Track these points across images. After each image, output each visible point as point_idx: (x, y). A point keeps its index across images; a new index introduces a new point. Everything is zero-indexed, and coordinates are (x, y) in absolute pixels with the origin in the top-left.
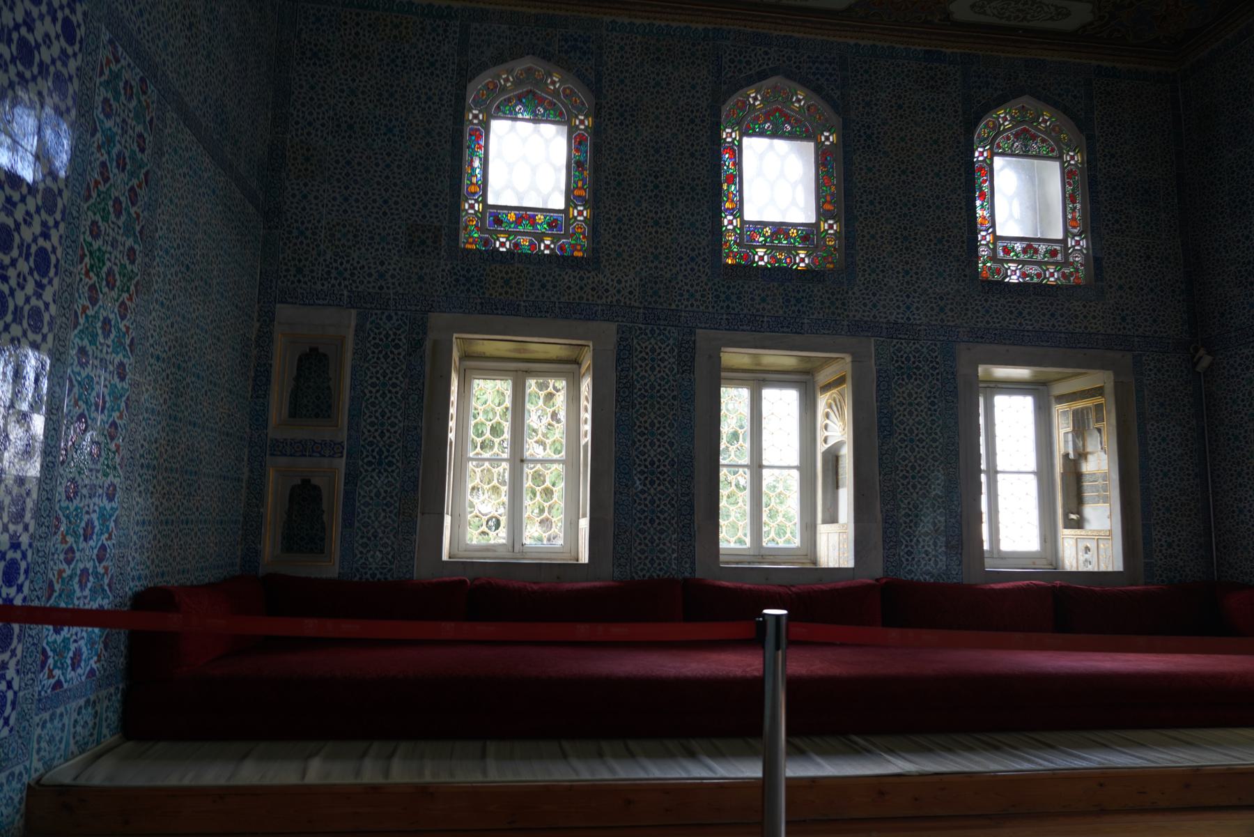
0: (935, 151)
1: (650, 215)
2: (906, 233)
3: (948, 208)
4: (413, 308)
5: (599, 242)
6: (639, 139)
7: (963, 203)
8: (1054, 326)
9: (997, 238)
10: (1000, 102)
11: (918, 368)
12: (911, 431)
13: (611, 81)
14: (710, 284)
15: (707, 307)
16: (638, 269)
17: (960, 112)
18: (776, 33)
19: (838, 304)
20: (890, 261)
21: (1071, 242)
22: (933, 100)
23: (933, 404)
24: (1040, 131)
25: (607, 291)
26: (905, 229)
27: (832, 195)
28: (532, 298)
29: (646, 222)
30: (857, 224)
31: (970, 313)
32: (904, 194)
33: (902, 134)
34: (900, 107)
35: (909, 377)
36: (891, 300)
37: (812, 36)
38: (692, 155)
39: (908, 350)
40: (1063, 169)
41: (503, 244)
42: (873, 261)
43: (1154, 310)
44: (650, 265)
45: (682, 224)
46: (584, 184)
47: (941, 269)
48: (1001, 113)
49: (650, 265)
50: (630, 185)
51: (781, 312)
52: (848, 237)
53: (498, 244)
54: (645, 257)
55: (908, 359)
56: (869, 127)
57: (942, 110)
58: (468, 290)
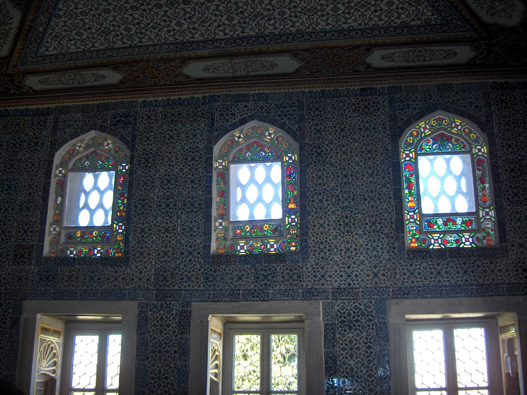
0: (369, 158)
1: (163, 225)
2: (347, 221)
3: (379, 199)
4: (15, 298)
5: (128, 247)
6: (157, 175)
7: (391, 194)
9: (422, 216)
10: (420, 116)
13: (141, 139)
14: (202, 270)
15: (199, 286)
16: (153, 263)
18: (252, 93)
19: (295, 277)
20: (335, 242)
22: (367, 122)
23: (369, 347)
24: (453, 133)
25: (132, 279)
26: (347, 217)
27: (295, 197)
28: (85, 288)
29: (160, 230)
30: (310, 217)
31: (398, 276)
32: (346, 192)
33: (344, 149)
34: (342, 130)
37: (278, 91)
38: (192, 181)
39: (349, 308)
40: (473, 159)
41: (72, 252)
42: (322, 243)
44: (162, 259)
45: (184, 229)
46: (124, 208)
47: (375, 245)
48: (422, 124)
49: (162, 259)
50: (150, 206)
51: (252, 286)
52: (303, 229)
53: (69, 252)
54: (159, 255)
55: (349, 315)
56: (319, 147)
57: (374, 128)
58: (47, 285)
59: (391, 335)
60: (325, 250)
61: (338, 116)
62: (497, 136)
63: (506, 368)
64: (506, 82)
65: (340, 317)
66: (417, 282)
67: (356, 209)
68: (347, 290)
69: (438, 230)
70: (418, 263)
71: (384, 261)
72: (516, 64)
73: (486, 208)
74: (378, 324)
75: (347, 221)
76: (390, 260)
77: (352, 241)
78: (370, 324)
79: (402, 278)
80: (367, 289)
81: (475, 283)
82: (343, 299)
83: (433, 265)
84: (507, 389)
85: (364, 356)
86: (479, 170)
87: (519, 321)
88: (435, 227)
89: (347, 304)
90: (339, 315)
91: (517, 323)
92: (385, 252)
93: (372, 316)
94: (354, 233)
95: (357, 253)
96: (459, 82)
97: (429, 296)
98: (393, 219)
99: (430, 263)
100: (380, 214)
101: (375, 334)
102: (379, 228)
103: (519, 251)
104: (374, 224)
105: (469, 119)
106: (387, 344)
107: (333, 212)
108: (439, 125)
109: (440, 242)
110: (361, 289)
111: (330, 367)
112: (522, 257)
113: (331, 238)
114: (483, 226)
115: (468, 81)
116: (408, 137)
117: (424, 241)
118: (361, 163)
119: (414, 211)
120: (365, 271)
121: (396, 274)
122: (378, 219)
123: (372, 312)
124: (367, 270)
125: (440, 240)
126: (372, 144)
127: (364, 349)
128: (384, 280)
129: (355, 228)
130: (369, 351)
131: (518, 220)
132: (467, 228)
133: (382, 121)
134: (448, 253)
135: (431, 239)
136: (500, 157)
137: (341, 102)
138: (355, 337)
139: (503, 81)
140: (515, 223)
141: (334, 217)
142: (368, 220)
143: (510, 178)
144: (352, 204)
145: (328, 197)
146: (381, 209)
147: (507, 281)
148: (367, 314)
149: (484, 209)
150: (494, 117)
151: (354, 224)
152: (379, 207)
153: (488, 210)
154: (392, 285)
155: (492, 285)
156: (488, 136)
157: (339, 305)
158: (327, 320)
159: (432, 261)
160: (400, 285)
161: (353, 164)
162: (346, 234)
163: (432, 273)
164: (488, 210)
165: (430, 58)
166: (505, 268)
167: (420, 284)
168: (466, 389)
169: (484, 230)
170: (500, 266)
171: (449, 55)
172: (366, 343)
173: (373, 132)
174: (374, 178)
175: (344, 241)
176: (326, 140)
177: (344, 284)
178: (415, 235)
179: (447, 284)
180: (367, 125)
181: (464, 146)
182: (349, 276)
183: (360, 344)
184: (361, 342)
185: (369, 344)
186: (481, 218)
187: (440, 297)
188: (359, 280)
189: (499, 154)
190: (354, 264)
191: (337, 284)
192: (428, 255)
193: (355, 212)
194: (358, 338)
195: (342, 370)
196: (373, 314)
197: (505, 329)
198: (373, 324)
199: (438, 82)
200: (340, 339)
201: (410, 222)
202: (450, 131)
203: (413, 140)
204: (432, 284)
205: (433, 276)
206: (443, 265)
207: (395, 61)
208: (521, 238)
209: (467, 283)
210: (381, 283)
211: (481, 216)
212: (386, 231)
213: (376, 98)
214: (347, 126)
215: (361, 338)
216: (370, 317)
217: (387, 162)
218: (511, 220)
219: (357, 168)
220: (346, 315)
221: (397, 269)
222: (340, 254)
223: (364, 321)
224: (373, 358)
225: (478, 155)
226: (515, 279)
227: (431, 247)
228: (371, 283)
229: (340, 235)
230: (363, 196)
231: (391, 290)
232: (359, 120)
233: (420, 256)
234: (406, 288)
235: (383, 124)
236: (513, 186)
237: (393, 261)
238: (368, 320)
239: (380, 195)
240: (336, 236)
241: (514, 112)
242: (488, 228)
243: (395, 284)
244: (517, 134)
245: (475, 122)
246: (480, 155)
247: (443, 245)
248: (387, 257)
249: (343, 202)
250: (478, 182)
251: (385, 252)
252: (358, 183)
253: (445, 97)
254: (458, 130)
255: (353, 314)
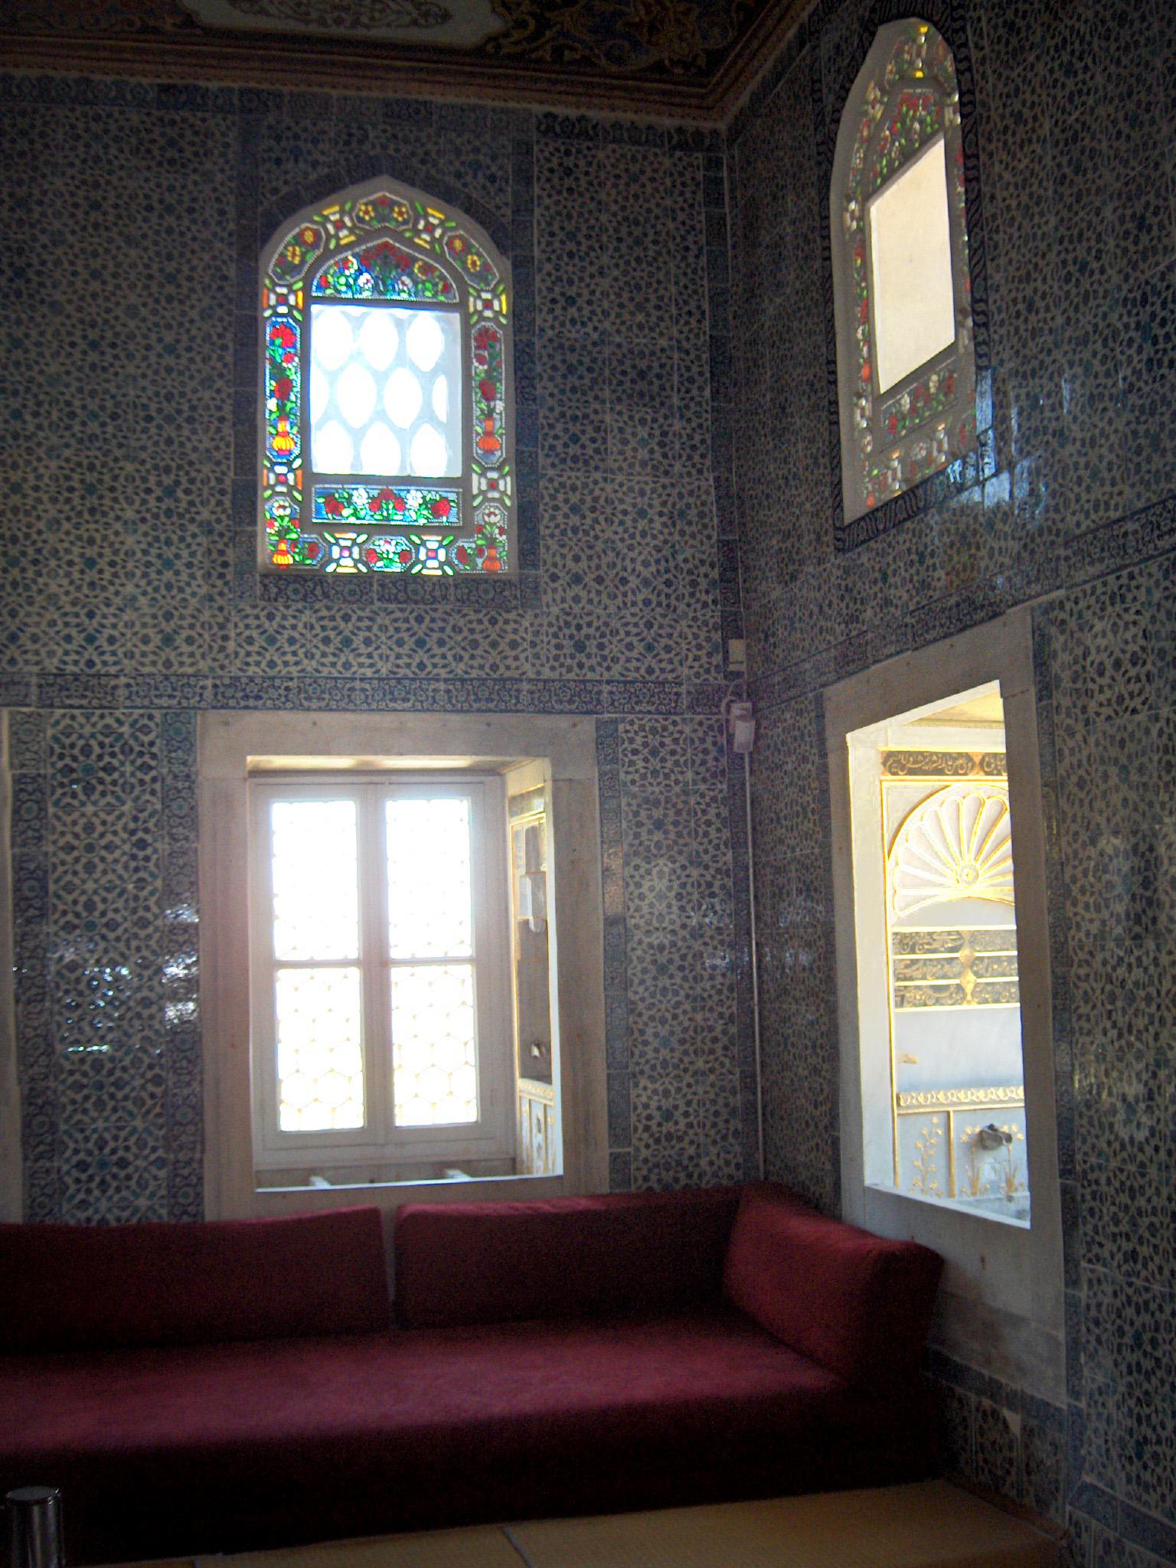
2: (90, 478)
3: (190, 420)
7: (227, 410)
8: (422, 666)
9: (309, 477)
10: (327, 188)
11: (109, 769)
12: (90, 906)
17: (232, 213)
21: (478, 484)
22: (171, 189)
23: (142, 844)
24: (419, 248)
26: (91, 468)
31: (231, 646)
32: (93, 394)
33: (96, 264)
35: (89, 790)
36: (52, 623)
39: (88, 730)
43: (649, 625)
47: (169, 553)
48: (333, 213)
55: (86, 750)
56: (20, 252)
59: (205, 809)
60: (24, 561)
61: (84, 161)
62: (540, 270)
63: (520, 910)
64: (582, 119)
65: (61, 757)
66: (286, 664)
67: (120, 446)
68: (84, 679)
69: (352, 520)
70: (290, 612)
71: (194, 602)
72: (614, 69)
73: (492, 469)
74: (169, 780)
75: (90, 478)
76: (211, 599)
77: (105, 538)
78: (147, 778)
79: (242, 652)
80: (140, 680)
81: (443, 673)
82: (71, 706)
83: (333, 618)
84: (520, 964)
85: (126, 867)
86: (481, 360)
87: (555, 781)
88: (346, 512)
89: (82, 720)
90: (58, 750)
91: (549, 785)
92: (199, 574)
93: (154, 756)
94: (112, 515)
95: (115, 575)
96: (451, 99)
97: (315, 704)
98: (228, 481)
99: (324, 613)
100: (191, 463)
101: (159, 807)
102: (184, 505)
103: (570, 594)
104: (170, 492)
105: (467, 211)
106: (192, 836)
107: (51, 449)
108: (381, 218)
109: (356, 556)
110: (123, 680)
111: (27, 899)
112: (577, 609)
113: (41, 525)
114: (478, 518)
115: (473, 101)
116: (285, 245)
117: (313, 549)
118: (144, 311)
119: (289, 464)
120: (137, 628)
121: (225, 638)
122: (184, 479)
123: (152, 744)
124: (144, 625)
125: (356, 550)
126: (182, 255)
127: (127, 847)
128: (192, 655)
129: (115, 500)
130: (141, 854)
131: (574, 509)
132: (435, 522)
133: (215, 190)
134: (375, 587)
135: (330, 545)
136: (542, 330)
137: (97, 118)
138: (103, 815)
139: (573, 113)
140: (566, 516)
141: (54, 464)
142: (153, 479)
143: (563, 392)
144: (110, 429)
145: (39, 404)
146: (195, 449)
147: (531, 675)
148: (137, 749)
149: (484, 471)
150: (537, 211)
151: (112, 489)
152: (189, 445)
153: (494, 475)
154: (212, 669)
155: (490, 683)
156: (515, 266)
157: (57, 723)
158: (22, 766)
159: (329, 609)
160: (235, 672)
161: (119, 311)
162: (86, 516)
163: (326, 641)
164: (494, 475)
165: (372, 18)
166: (529, 637)
167: (293, 669)
168: (413, 962)
169: (480, 529)
170: (515, 631)
171: (426, 15)
172: (133, 832)
173: (186, 222)
174: (178, 357)
175: (79, 538)
176: (43, 231)
177: (76, 663)
178: (288, 530)
179: (369, 672)
180: (170, 199)
181: (447, 289)
182: (91, 639)
183: (115, 833)
184: (119, 827)
185: (140, 834)
186: (474, 497)
187: (345, 710)
188: (120, 652)
189: (539, 322)
190: (108, 605)
191: (55, 661)
192: (318, 592)
193: (118, 453)
194: (110, 819)
195: (61, 907)
196: (154, 750)
197: (520, 802)
198: (154, 780)
199: (391, 95)
200: (58, 818)
201: (276, 494)
202: (411, 240)
203: (303, 255)
204: (325, 671)
205: (330, 649)
206: (360, 619)
207: (267, 14)
208: (577, 559)
209: (422, 675)
210: (182, 664)
211: (475, 491)
212: (205, 514)
213: (204, 120)
214: (112, 195)
215: (119, 817)
216: (147, 758)
217: (219, 312)
218: (556, 508)
219: (132, 324)
220: (76, 752)
221: (230, 625)
222: (68, 575)
223: (128, 768)
224: (152, 875)
225: (482, 318)
226: (553, 668)
227: (330, 569)
228: (154, 663)
229: (68, 519)
230: (145, 407)
231: (209, 682)
232: (147, 180)
233: (296, 591)
234: (251, 679)
235: (218, 200)
236: (569, 413)
237: (220, 601)
238: (140, 768)
239: (193, 408)
240: (58, 522)
241: (592, 206)
242: (491, 525)
243: (222, 667)
244: (593, 269)
245: (482, 223)
246: (488, 319)
247: (366, 564)
248: (203, 591)
249: (84, 424)
250: (477, 395)
251: (199, 574)
252: (131, 369)
253: (406, 141)
254: (434, 241)
255: (97, 750)
